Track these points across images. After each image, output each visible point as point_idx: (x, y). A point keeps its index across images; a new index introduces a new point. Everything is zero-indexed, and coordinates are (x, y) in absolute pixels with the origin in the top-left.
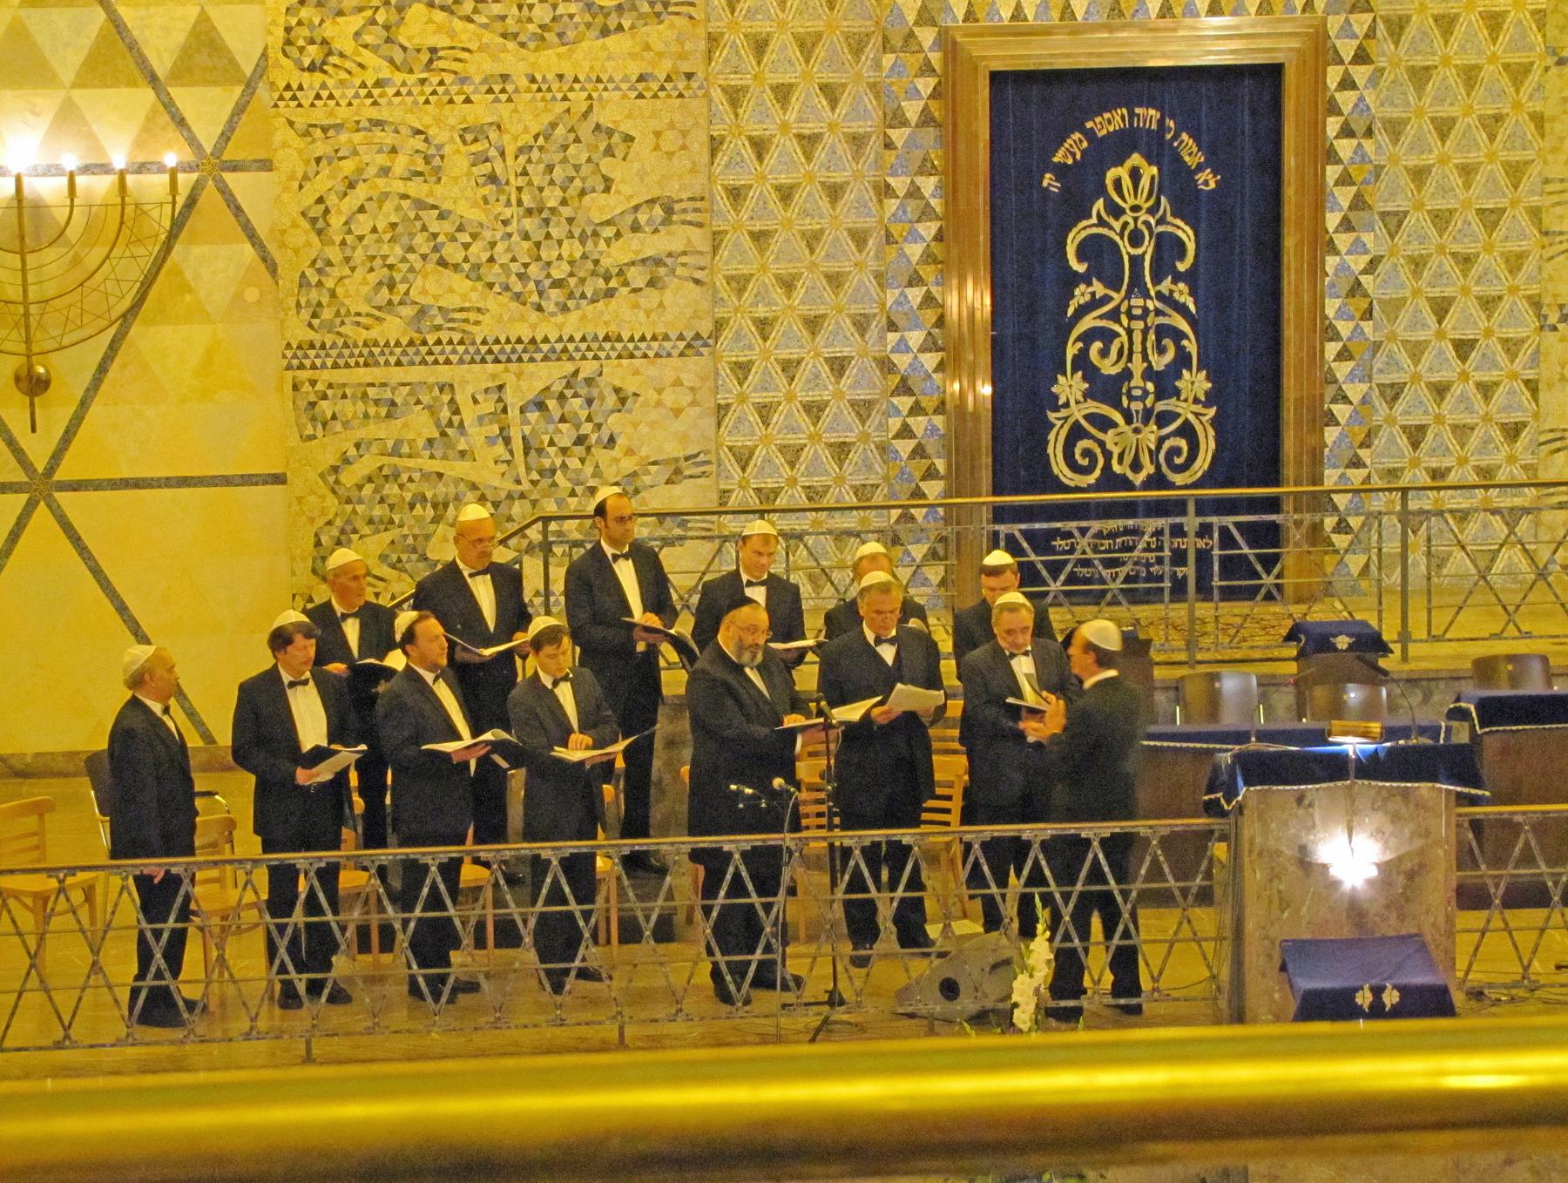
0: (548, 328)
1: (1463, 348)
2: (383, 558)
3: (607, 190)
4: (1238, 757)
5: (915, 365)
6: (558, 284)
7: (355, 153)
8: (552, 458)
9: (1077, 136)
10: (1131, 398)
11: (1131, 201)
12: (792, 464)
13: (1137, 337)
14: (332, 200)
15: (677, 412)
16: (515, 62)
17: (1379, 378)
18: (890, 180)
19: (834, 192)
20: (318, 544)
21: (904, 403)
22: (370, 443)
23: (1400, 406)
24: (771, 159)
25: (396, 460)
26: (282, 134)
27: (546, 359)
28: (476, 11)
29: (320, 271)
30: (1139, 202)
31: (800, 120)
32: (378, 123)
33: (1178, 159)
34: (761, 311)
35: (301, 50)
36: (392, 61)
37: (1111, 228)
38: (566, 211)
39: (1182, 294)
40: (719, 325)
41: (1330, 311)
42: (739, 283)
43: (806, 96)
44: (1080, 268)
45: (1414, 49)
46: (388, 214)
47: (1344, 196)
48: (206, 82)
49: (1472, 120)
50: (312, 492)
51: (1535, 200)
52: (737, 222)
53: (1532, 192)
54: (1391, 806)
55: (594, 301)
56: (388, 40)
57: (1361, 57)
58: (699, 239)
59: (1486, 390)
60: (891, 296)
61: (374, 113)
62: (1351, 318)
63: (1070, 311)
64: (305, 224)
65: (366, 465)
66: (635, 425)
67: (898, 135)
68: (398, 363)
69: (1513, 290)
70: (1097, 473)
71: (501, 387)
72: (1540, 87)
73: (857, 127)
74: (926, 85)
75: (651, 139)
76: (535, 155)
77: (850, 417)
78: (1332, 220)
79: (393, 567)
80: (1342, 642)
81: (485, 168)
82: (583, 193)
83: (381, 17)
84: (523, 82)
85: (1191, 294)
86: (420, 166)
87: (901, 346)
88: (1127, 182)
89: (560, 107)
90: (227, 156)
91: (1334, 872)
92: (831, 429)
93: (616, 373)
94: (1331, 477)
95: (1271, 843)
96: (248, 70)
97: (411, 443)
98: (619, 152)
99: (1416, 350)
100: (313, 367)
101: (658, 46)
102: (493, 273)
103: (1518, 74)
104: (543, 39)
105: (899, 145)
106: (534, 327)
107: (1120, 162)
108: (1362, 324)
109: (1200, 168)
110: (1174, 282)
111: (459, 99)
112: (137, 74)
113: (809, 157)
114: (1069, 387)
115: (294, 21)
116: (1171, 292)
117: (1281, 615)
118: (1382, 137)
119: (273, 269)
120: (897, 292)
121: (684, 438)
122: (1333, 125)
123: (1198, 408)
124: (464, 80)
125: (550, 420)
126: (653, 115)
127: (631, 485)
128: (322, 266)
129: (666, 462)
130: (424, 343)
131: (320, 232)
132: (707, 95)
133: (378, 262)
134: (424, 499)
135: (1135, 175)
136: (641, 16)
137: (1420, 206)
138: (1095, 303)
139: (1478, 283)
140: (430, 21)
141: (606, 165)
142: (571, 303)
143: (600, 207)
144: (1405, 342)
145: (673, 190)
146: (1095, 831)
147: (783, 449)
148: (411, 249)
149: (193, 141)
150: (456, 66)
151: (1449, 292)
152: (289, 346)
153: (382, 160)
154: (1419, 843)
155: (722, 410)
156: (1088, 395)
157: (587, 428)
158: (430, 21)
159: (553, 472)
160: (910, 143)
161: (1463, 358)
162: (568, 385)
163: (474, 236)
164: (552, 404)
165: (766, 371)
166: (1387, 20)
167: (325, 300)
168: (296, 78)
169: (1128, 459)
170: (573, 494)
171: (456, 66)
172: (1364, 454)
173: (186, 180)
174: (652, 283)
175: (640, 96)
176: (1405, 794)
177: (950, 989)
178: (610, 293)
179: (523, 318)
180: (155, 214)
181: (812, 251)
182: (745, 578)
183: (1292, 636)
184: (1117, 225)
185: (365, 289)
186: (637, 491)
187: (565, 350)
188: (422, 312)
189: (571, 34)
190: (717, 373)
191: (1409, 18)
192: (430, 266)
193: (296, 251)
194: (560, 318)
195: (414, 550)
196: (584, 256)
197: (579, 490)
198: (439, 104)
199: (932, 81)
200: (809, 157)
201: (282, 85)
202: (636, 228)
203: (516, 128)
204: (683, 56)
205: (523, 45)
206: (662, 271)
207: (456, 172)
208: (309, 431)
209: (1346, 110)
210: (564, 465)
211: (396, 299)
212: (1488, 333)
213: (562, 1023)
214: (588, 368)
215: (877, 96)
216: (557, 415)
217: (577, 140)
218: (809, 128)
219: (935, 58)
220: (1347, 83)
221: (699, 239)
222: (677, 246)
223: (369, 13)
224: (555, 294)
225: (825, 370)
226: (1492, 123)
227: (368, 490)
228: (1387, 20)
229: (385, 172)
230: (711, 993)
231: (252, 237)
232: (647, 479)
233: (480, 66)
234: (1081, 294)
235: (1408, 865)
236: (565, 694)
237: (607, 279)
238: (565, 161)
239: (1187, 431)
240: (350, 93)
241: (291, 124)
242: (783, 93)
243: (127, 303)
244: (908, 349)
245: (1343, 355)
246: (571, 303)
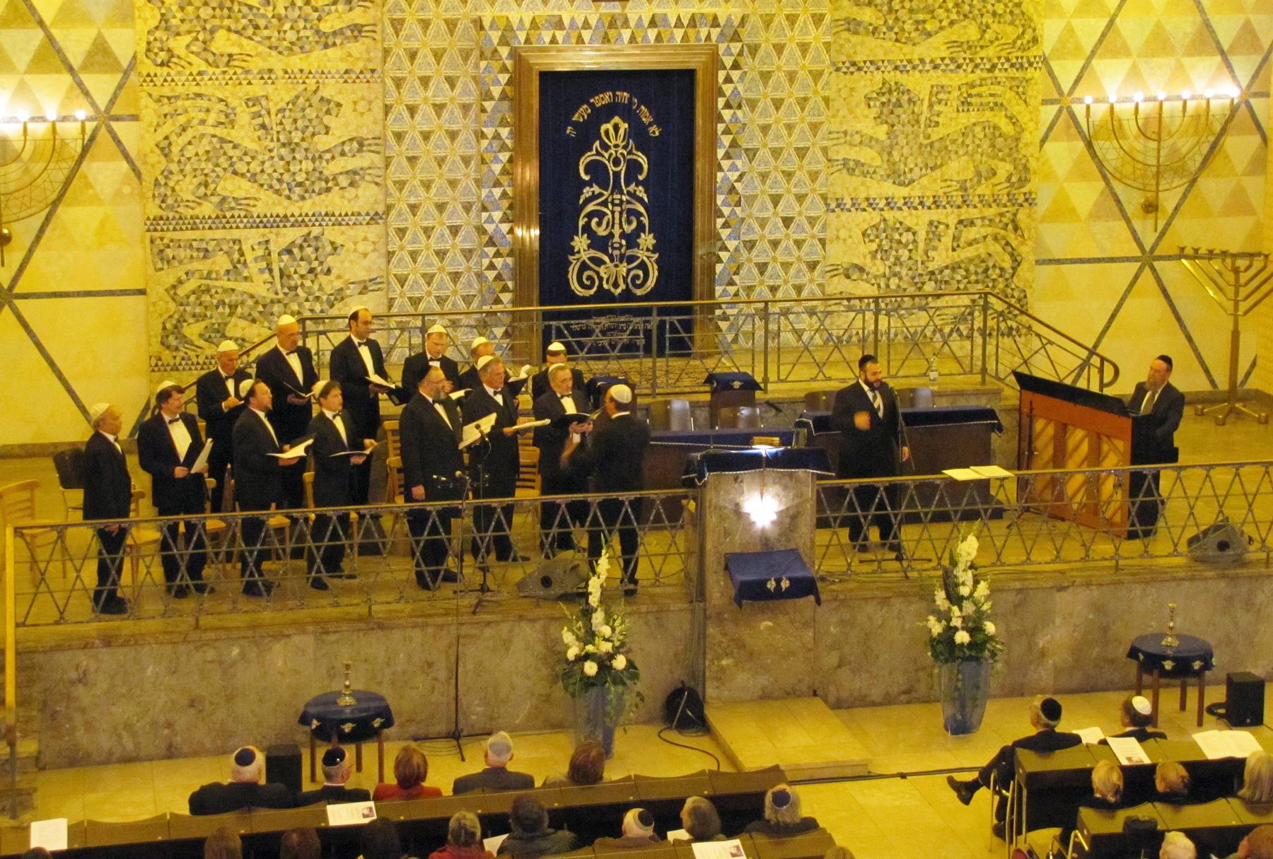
0: (295, 209)
1: (787, 221)
2: (201, 336)
3: (327, 133)
4: (704, 457)
5: (497, 230)
6: (300, 184)
7: (186, 111)
8: (296, 280)
9: (585, 106)
10: (614, 248)
11: (614, 142)
12: (429, 284)
13: (617, 215)
14: (173, 138)
15: (365, 255)
16: (277, 62)
17: (743, 238)
18: (485, 130)
19: (453, 135)
20: (164, 328)
21: (491, 251)
22: (193, 273)
23: (754, 252)
24: (418, 117)
25: (208, 282)
26: (145, 101)
27: (293, 226)
28: (254, 34)
29: (166, 177)
30: (619, 142)
31: (434, 96)
32: (199, 95)
34: (412, 200)
35: (156, 54)
36: (207, 61)
38: (305, 145)
39: (641, 192)
40: (389, 208)
41: (719, 202)
42: (401, 185)
43: (438, 82)
44: (586, 178)
45: (763, 62)
46: (205, 145)
47: (726, 140)
48: (100, 72)
49: (792, 100)
50: (161, 299)
51: (825, 143)
52: (399, 152)
53: (823, 139)
54: (783, 481)
55: (319, 194)
56: (205, 50)
57: (736, 66)
58: (378, 160)
59: (799, 244)
60: (484, 192)
61: (197, 90)
64: (158, 151)
65: (192, 284)
66: (342, 262)
67: (489, 105)
68: (210, 228)
69: (813, 190)
70: (595, 289)
71: (267, 242)
72: (827, 83)
73: (466, 100)
74: (504, 78)
75: (351, 106)
76: (287, 113)
77: (461, 258)
78: (720, 153)
79: (206, 340)
80: (737, 384)
81: (259, 121)
82: (313, 135)
83: (201, 37)
84: (280, 74)
86: (223, 119)
87: (490, 220)
88: (612, 132)
89: (301, 87)
90: (113, 112)
91: (753, 518)
92: (450, 264)
93: (332, 234)
94: (719, 290)
95: (722, 503)
96: (125, 64)
97: (217, 272)
98: (334, 112)
99: (763, 223)
100: (162, 230)
101: (356, 54)
102: (263, 178)
103: (817, 76)
104: (291, 49)
106: (286, 208)
107: (608, 121)
109: (651, 124)
111: (245, 82)
112: (62, 66)
113: (439, 116)
114: (580, 242)
115: (152, 39)
117: (698, 368)
118: (746, 108)
119: (139, 175)
121: (369, 270)
122: (721, 102)
123: (649, 254)
124: (247, 72)
125: (295, 259)
126: (354, 92)
127: (339, 295)
128: (168, 174)
129: (360, 282)
130: (225, 217)
131: (166, 156)
132: (383, 82)
133: (199, 172)
134: (224, 303)
135: (616, 128)
136: (347, 38)
137: (765, 146)
138: (594, 197)
139: (795, 186)
140: (228, 39)
141: (326, 120)
142: (307, 195)
143: (323, 142)
144: (757, 218)
145: (364, 133)
146: (626, 496)
147: (424, 276)
148: (217, 165)
149: (93, 104)
150: (243, 64)
151: (780, 191)
152: (148, 219)
153: (202, 115)
154: (797, 501)
155: (390, 255)
156: (590, 246)
157: (315, 264)
158: (228, 39)
159: (296, 288)
160: (495, 109)
161: (787, 226)
162: (305, 240)
163: (253, 158)
164: (296, 251)
165: (415, 234)
166: (749, 46)
167: (169, 193)
168: (153, 70)
169: (612, 281)
170: (307, 300)
171: (243, 64)
172: (736, 278)
173: (90, 126)
174: (352, 184)
175: (346, 82)
176: (791, 475)
177: (546, 582)
178: (328, 190)
179: (280, 203)
180: (72, 145)
181: (440, 166)
182: (429, 356)
183: (710, 379)
184: (606, 155)
185: (192, 187)
186: (342, 299)
187: (303, 221)
188: (224, 199)
189: (307, 47)
190: (387, 234)
192: (228, 174)
193: (153, 166)
194: (301, 203)
195: (218, 331)
196: (314, 170)
197: (311, 298)
198: (234, 85)
199: (507, 76)
200: (439, 116)
201: (145, 73)
202: (343, 154)
203: (276, 98)
204: (369, 60)
205: (280, 53)
206: (357, 177)
207: (242, 123)
208: (160, 265)
209: (728, 93)
210: (302, 285)
211: (209, 193)
212: (800, 214)
213: (337, 605)
214: (316, 231)
215: (477, 83)
216: (298, 257)
217: (310, 106)
218: (439, 100)
219: (509, 63)
220: (728, 80)
221: (378, 160)
222: (366, 164)
223: (194, 34)
224: (298, 190)
225: (447, 232)
226: (803, 102)
227: (192, 298)
228: (749, 46)
229: (203, 122)
230: (415, 583)
231: (127, 157)
232: (348, 292)
233: (256, 64)
234: (587, 192)
235: (791, 512)
236: (339, 424)
237: (327, 182)
238: (304, 117)
239: (643, 266)
240: (183, 78)
241: (150, 95)
242: (425, 81)
243: (54, 196)
244: (493, 222)
245: (726, 225)
246: (307, 195)
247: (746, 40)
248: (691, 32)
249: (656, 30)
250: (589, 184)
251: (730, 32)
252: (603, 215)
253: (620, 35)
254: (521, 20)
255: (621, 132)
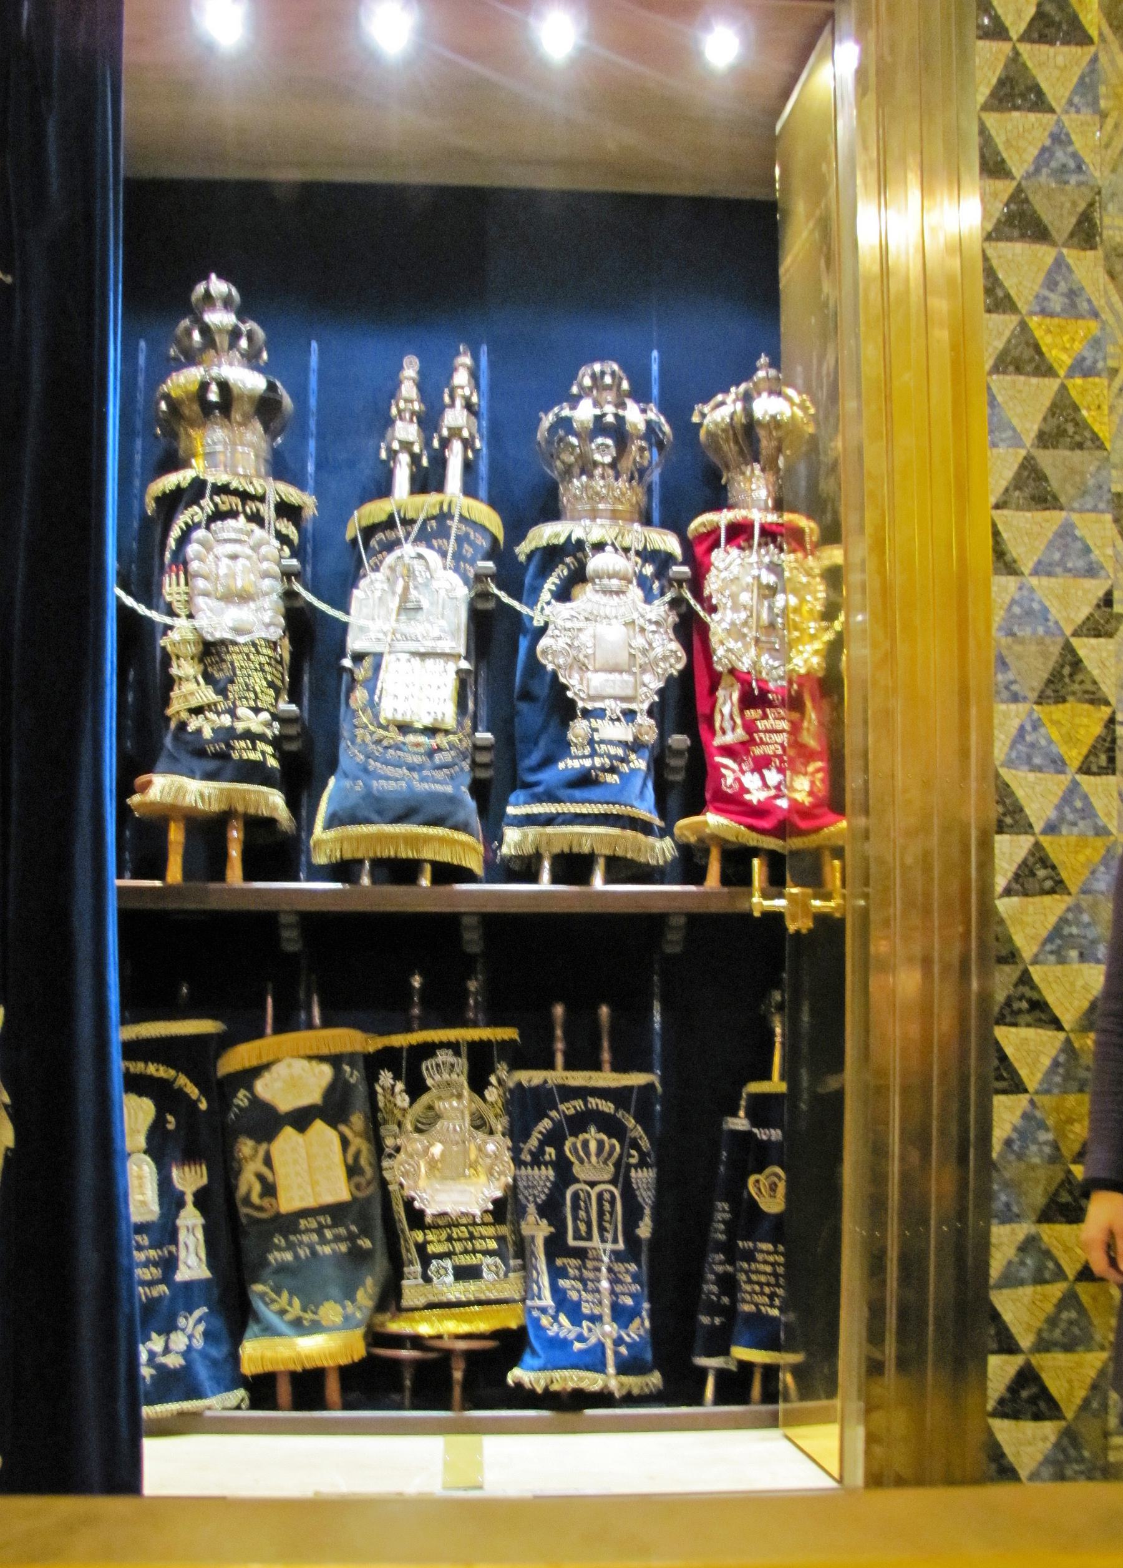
62: (1058, 764)
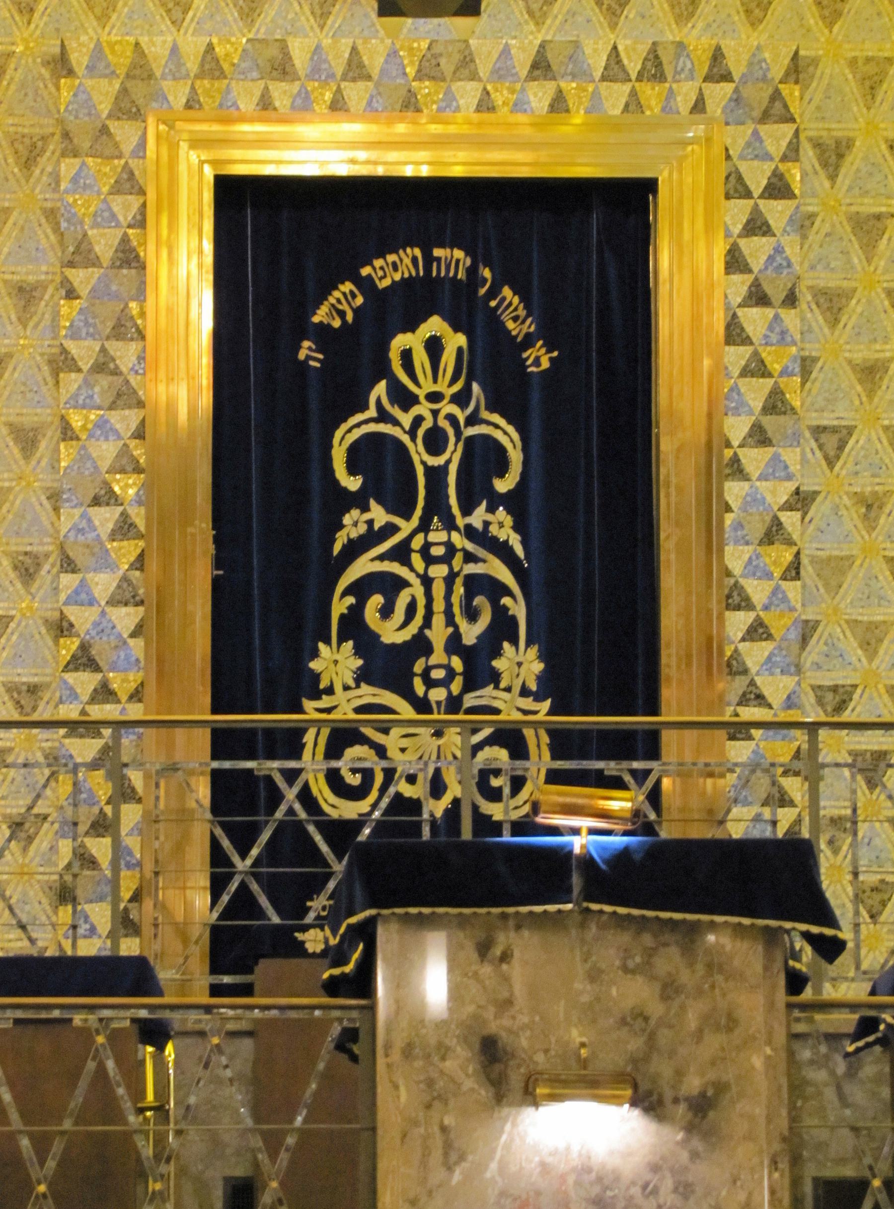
5: (102, 627)
10: (430, 683)
11: (428, 386)
13: (438, 589)
18: (72, 347)
33: (494, 321)
37: (396, 423)
44: (353, 484)
60: (69, 517)
62: (769, 576)
63: (337, 548)
67: (80, 277)
85: (516, 528)
88: (421, 358)
105: (84, 291)
107: (411, 326)
108: (785, 585)
109: (528, 341)
110: (491, 509)
116: (487, 524)
120: (77, 512)
123: (527, 703)
135: (434, 346)
138: (373, 537)
144: (853, 624)
156: (363, 677)
191: (850, 143)
209: (757, 263)
244: (92, 602)
247: (812, 128)
248: (651, 93)
249: (550, 88)
250: (360, 501)
251: (759, 96)
252: (396, 584)
253: (450, 97)
254: (175, 50)
255: (448, 358)
